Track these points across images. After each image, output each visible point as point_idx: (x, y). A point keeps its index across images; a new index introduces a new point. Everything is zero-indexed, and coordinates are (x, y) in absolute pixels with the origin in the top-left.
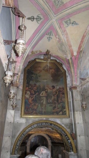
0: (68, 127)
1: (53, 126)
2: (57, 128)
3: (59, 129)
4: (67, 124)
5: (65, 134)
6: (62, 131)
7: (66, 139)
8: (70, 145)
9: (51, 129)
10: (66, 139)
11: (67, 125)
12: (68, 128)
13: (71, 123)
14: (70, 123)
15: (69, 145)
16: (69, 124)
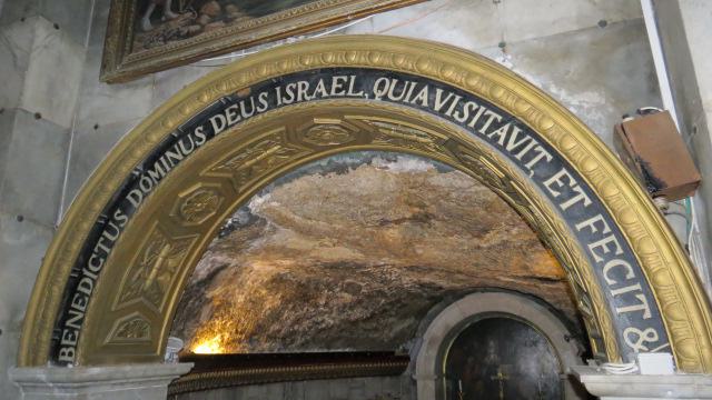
0: (575, 66)
1: (385, 98)
2: (430, 109)
3: (459, 108)
4: (566, 35)
5: (533, 153)
6: (496, 125)
7: (557, 202)
8: (618, 273)
9: (423, 166)
10: (561, 200)
11: (567, 54)
12: (576, 86)
13: (615, 17)
14: (603, 24)
15: (597, 268)
16: (584, 38)
